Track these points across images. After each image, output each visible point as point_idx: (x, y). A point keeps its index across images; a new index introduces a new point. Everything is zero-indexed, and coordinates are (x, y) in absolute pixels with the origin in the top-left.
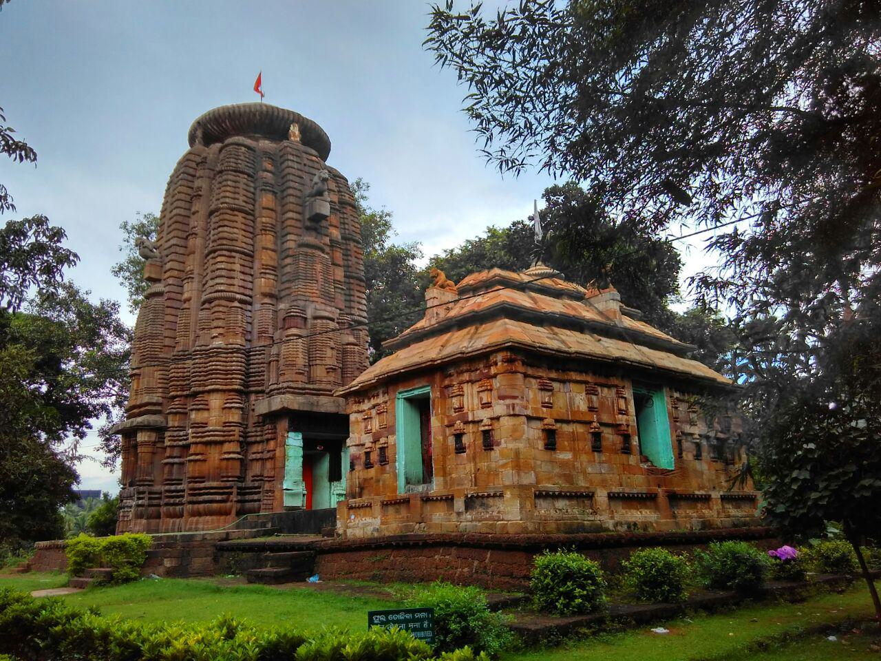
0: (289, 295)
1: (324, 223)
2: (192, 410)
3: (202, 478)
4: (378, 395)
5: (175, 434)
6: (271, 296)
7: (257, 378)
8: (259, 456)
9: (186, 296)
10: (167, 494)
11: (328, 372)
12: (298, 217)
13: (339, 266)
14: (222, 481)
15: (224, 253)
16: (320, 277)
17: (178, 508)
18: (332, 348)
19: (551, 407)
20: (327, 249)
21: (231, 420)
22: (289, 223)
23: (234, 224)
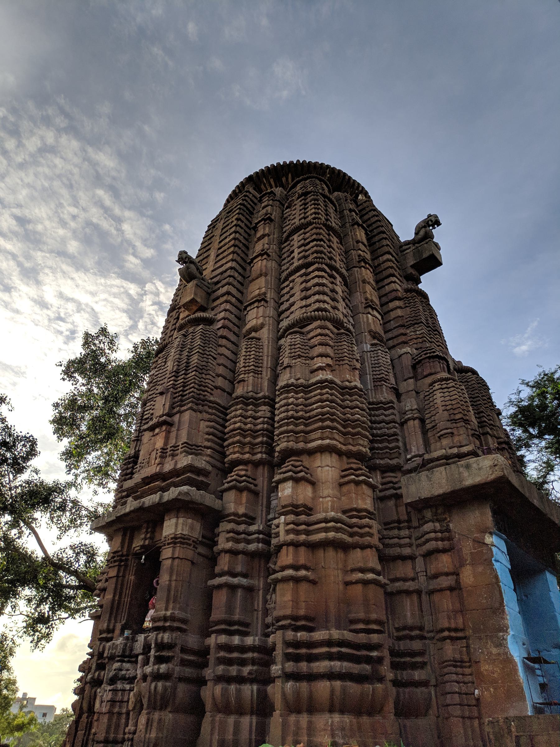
2: (285, 480)
3: (309, 622)
10: (222, 654)
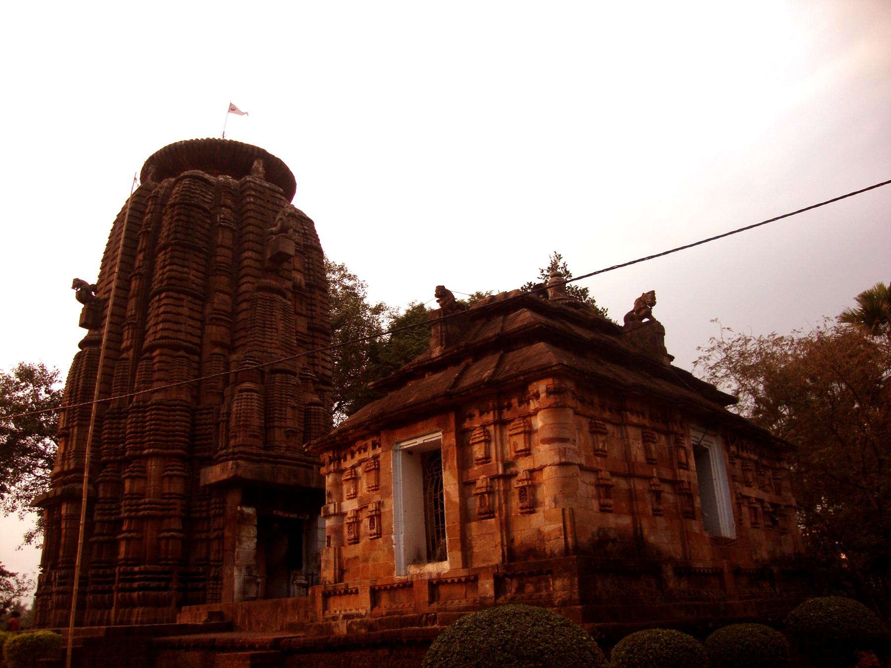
0: (244, 345)
1: (286, 265)
4: (365, 450)
5: (107, 506)
6: (222, 345)
7: (204, 442)
8: (203, 536)
9: (124, 345)
11: (288, 436)
12: (258, 256)
13: (301, 315)
14: (160, 565)
15: (171, 294)
16: (281, 326)
17: (107, 596)
18: (293, 408)
19: (605, 457)
20: (290, 295)
21: (172, 491)
22: (246, 263)
23: (186, 263)
